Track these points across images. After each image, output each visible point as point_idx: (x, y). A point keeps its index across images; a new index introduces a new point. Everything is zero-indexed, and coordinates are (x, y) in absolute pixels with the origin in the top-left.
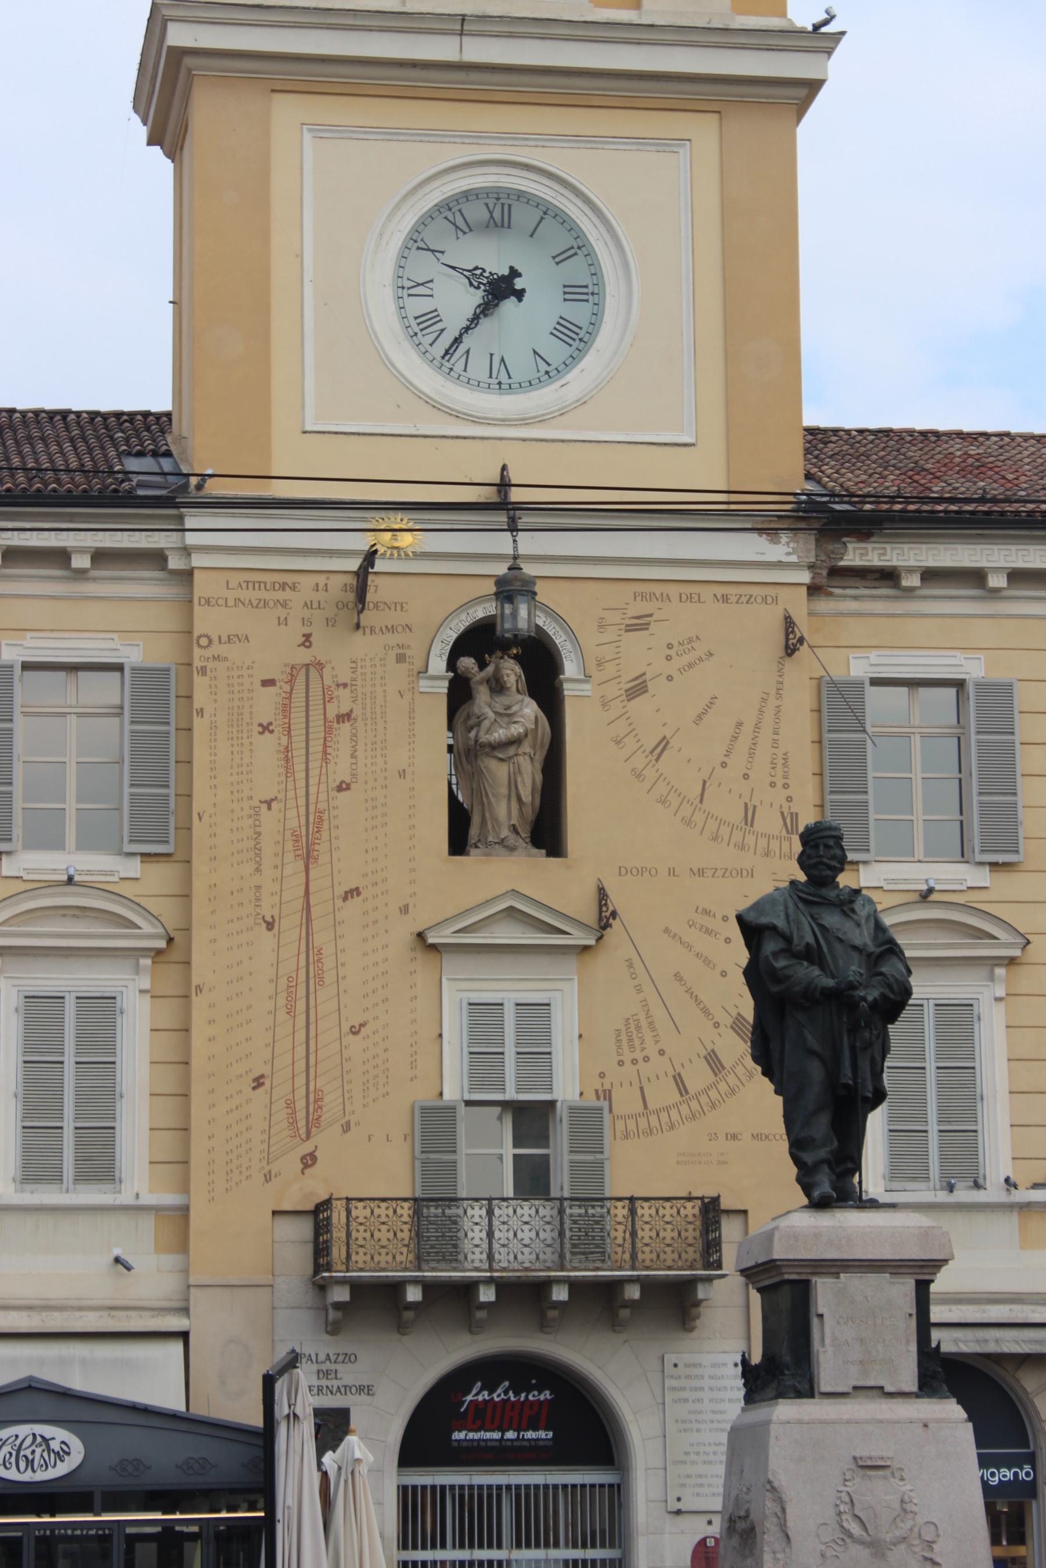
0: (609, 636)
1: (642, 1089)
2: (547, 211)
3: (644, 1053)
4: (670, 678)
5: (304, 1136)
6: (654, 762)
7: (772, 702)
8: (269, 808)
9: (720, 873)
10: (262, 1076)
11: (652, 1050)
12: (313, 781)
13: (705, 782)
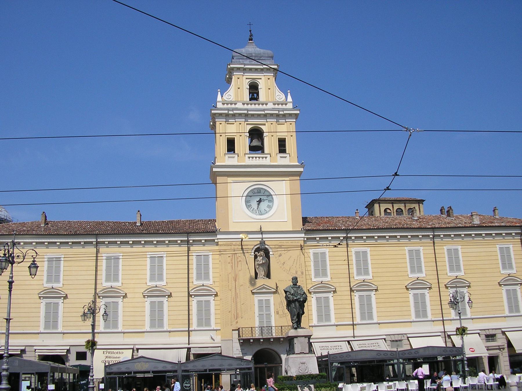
2: (265, 190)
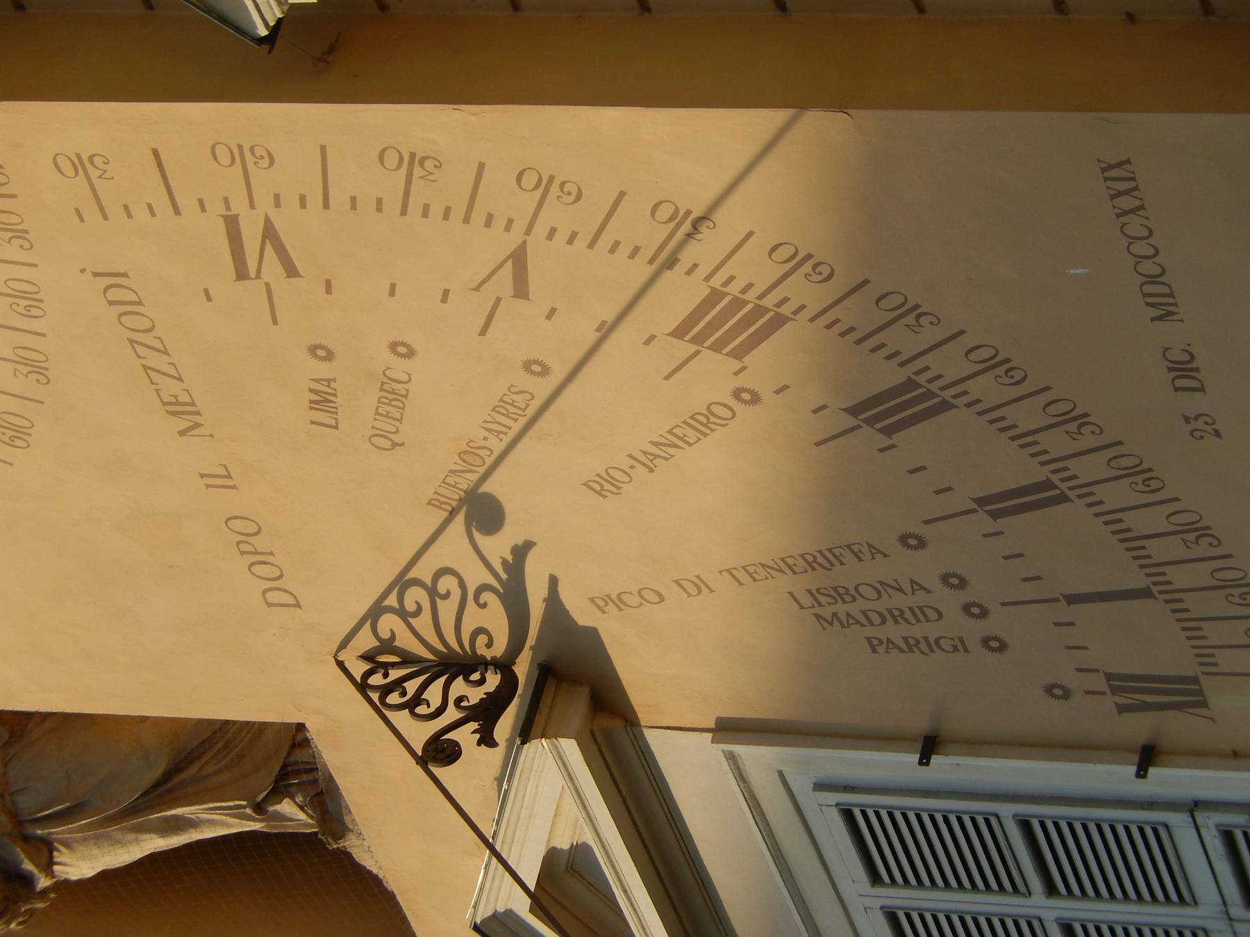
1: (1072, 599)
3: (934, 583)
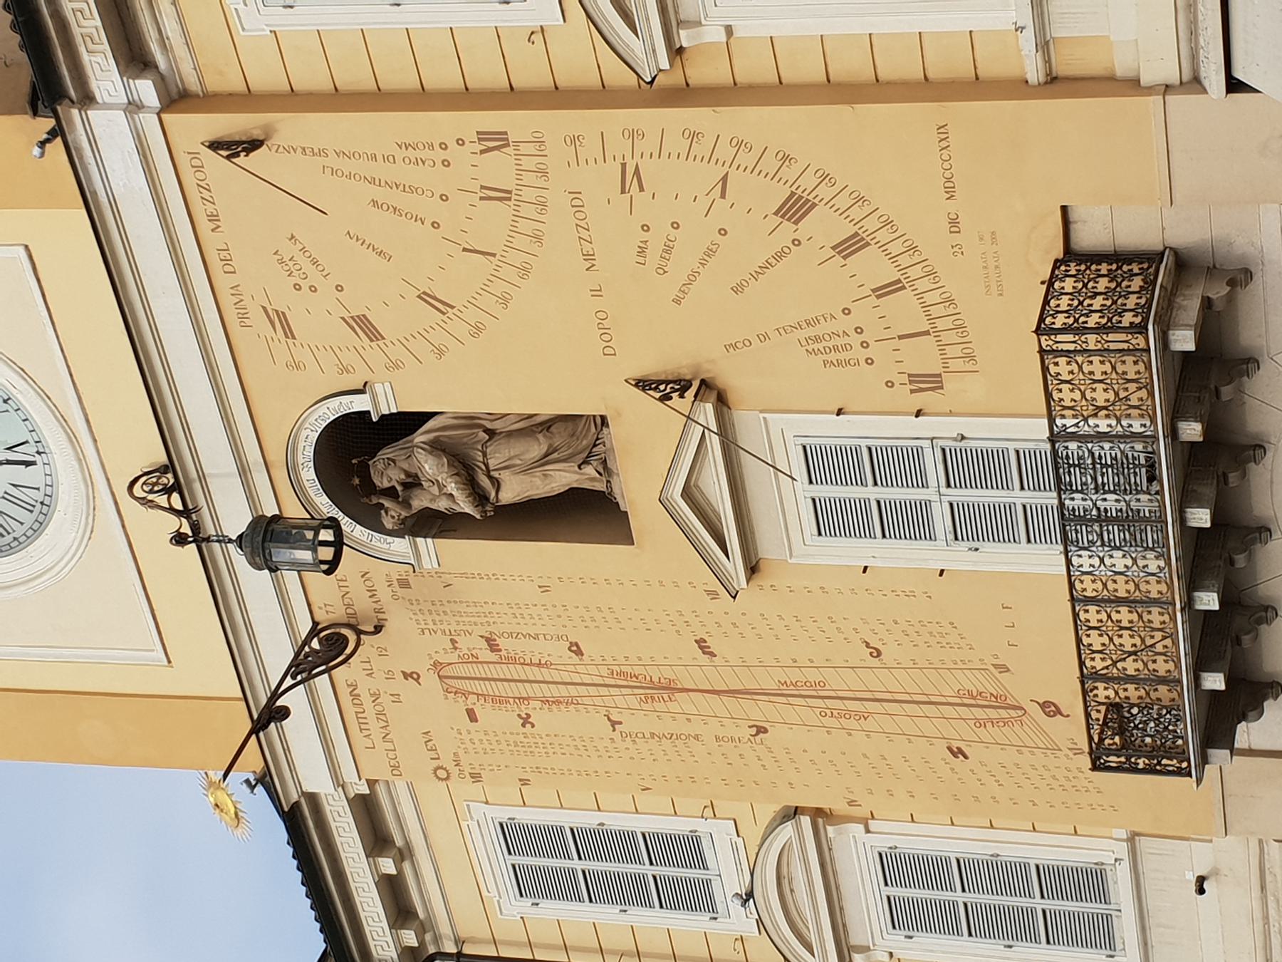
0: (304, 356)
1: (900, 337)
4: (339, 288)
5: (1020, 713)
6: (455, 311)
7: (332, 161)
8: (620, 723)
9: (584, 234)
10: (950, 749)
11: (847, 323)
12: (577, 679)
13: (465, 250)
